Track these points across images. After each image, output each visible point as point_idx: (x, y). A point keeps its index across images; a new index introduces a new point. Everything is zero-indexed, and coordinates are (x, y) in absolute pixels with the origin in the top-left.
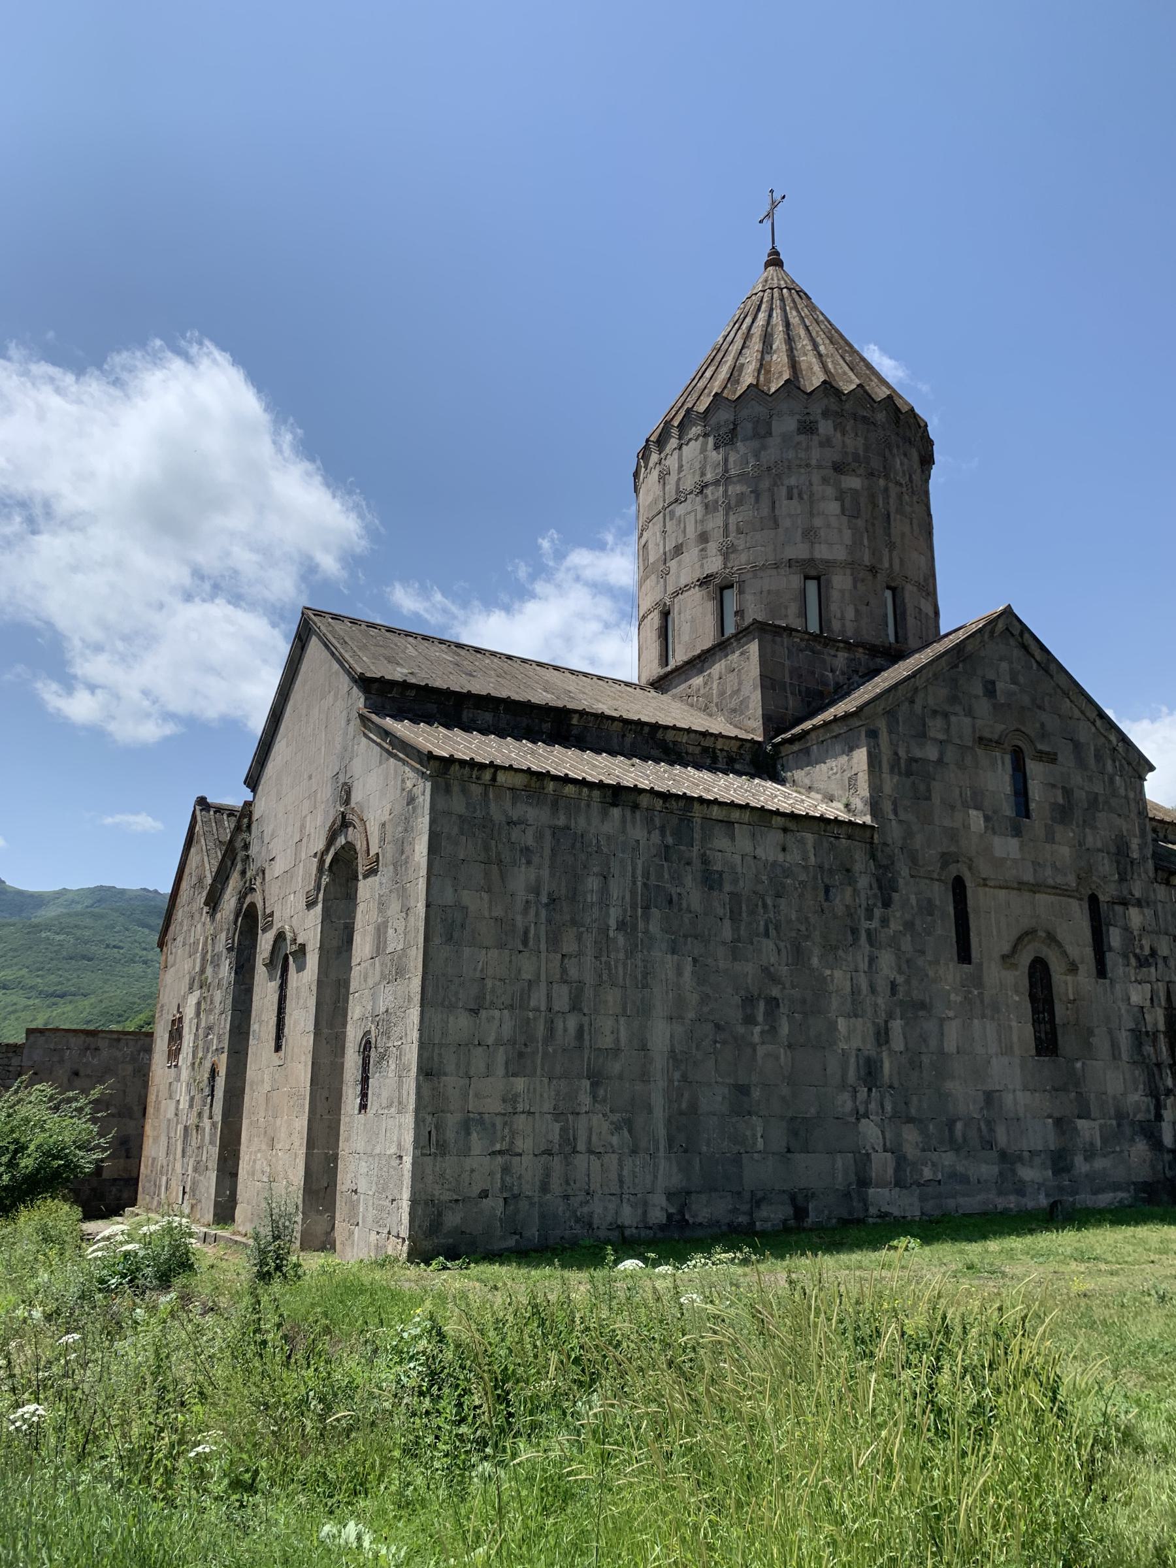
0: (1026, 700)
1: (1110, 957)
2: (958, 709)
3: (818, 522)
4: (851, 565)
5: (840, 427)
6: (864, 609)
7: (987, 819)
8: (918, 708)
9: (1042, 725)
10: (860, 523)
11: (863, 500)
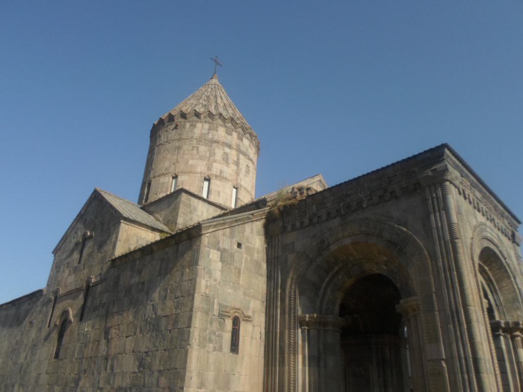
1: (86, 311)
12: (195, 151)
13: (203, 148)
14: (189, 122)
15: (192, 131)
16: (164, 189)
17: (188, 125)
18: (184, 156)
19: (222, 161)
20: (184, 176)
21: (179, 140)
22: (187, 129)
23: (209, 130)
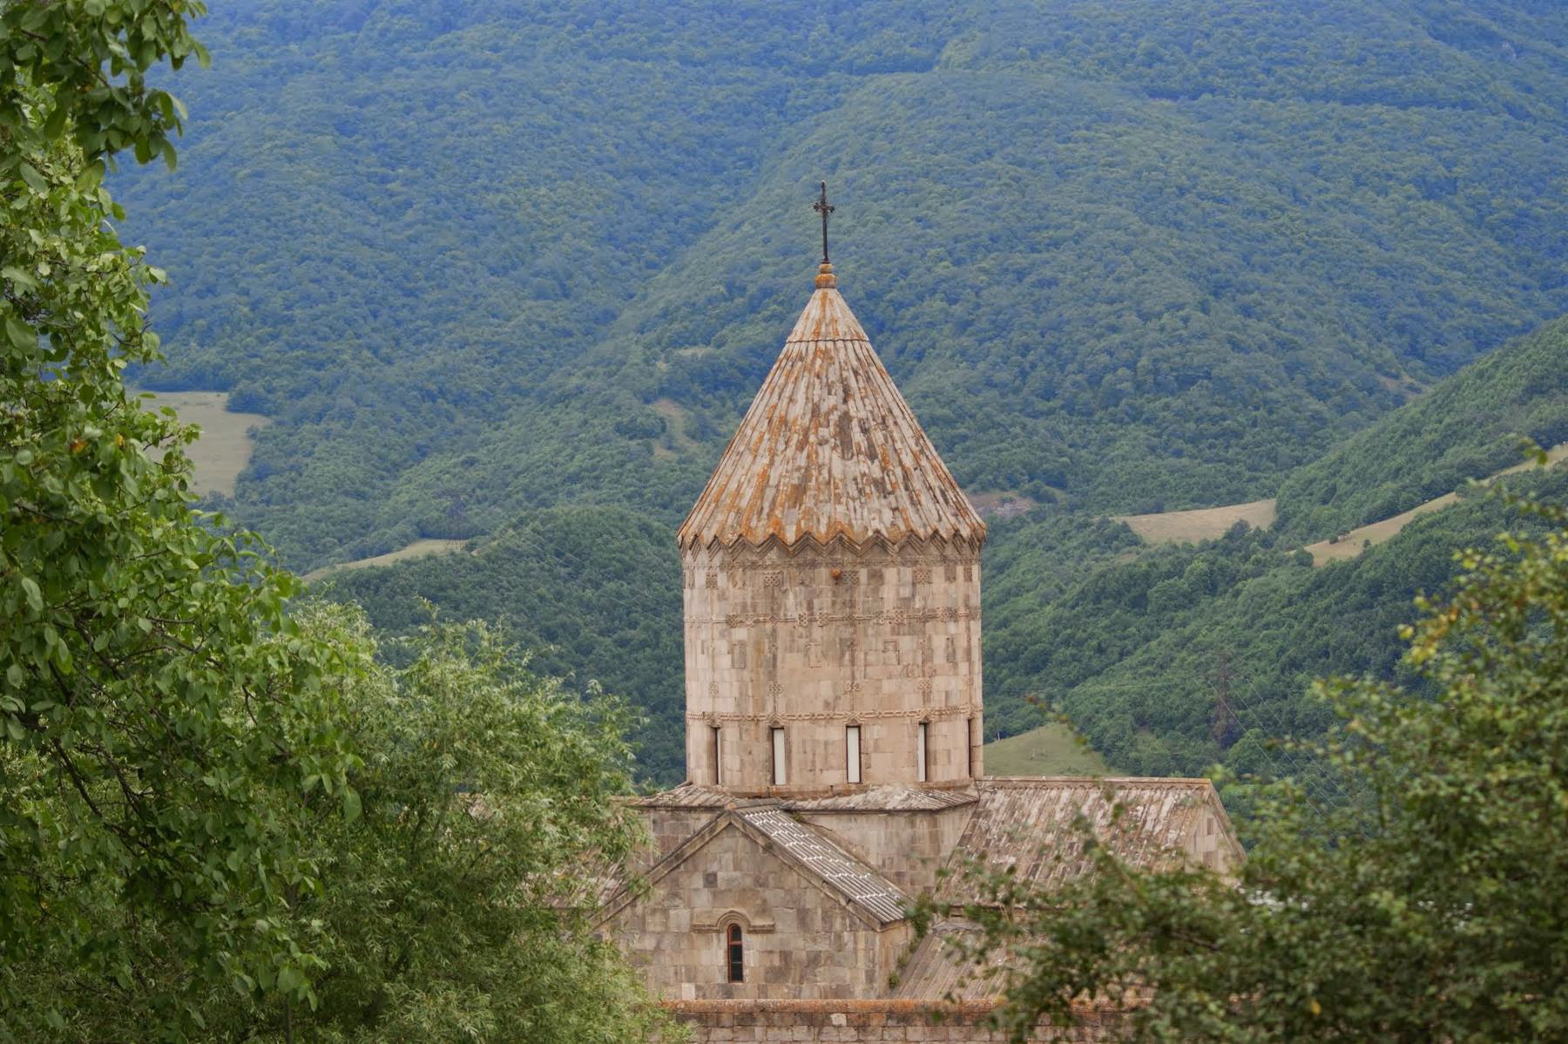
0: (749, 881)
2: (677, 902)
3: (717, 677)
4: (740, 719)
5: (731, 577)
6: (747, 758)
7: (698, 988)
8: (639, 909)
9: (765, 901)
10: (746, 674)
11: (749, 650)
12: (892, 655)
13: (906, 643)
14: (867, 564)
15: (876, 591)
16: (833, 761)
17: (863, 574)
18: (869, 669)
19: (948, 666)
20: (876, 728)
21: (851, 621)
22: (862, 588)
23: (914, 584)
